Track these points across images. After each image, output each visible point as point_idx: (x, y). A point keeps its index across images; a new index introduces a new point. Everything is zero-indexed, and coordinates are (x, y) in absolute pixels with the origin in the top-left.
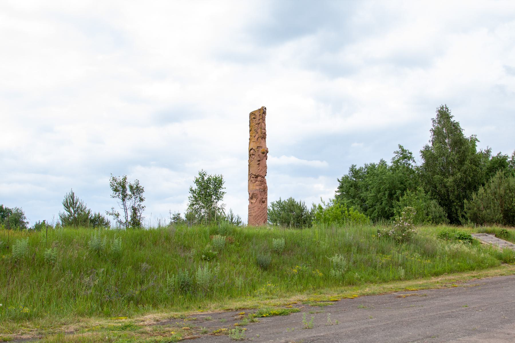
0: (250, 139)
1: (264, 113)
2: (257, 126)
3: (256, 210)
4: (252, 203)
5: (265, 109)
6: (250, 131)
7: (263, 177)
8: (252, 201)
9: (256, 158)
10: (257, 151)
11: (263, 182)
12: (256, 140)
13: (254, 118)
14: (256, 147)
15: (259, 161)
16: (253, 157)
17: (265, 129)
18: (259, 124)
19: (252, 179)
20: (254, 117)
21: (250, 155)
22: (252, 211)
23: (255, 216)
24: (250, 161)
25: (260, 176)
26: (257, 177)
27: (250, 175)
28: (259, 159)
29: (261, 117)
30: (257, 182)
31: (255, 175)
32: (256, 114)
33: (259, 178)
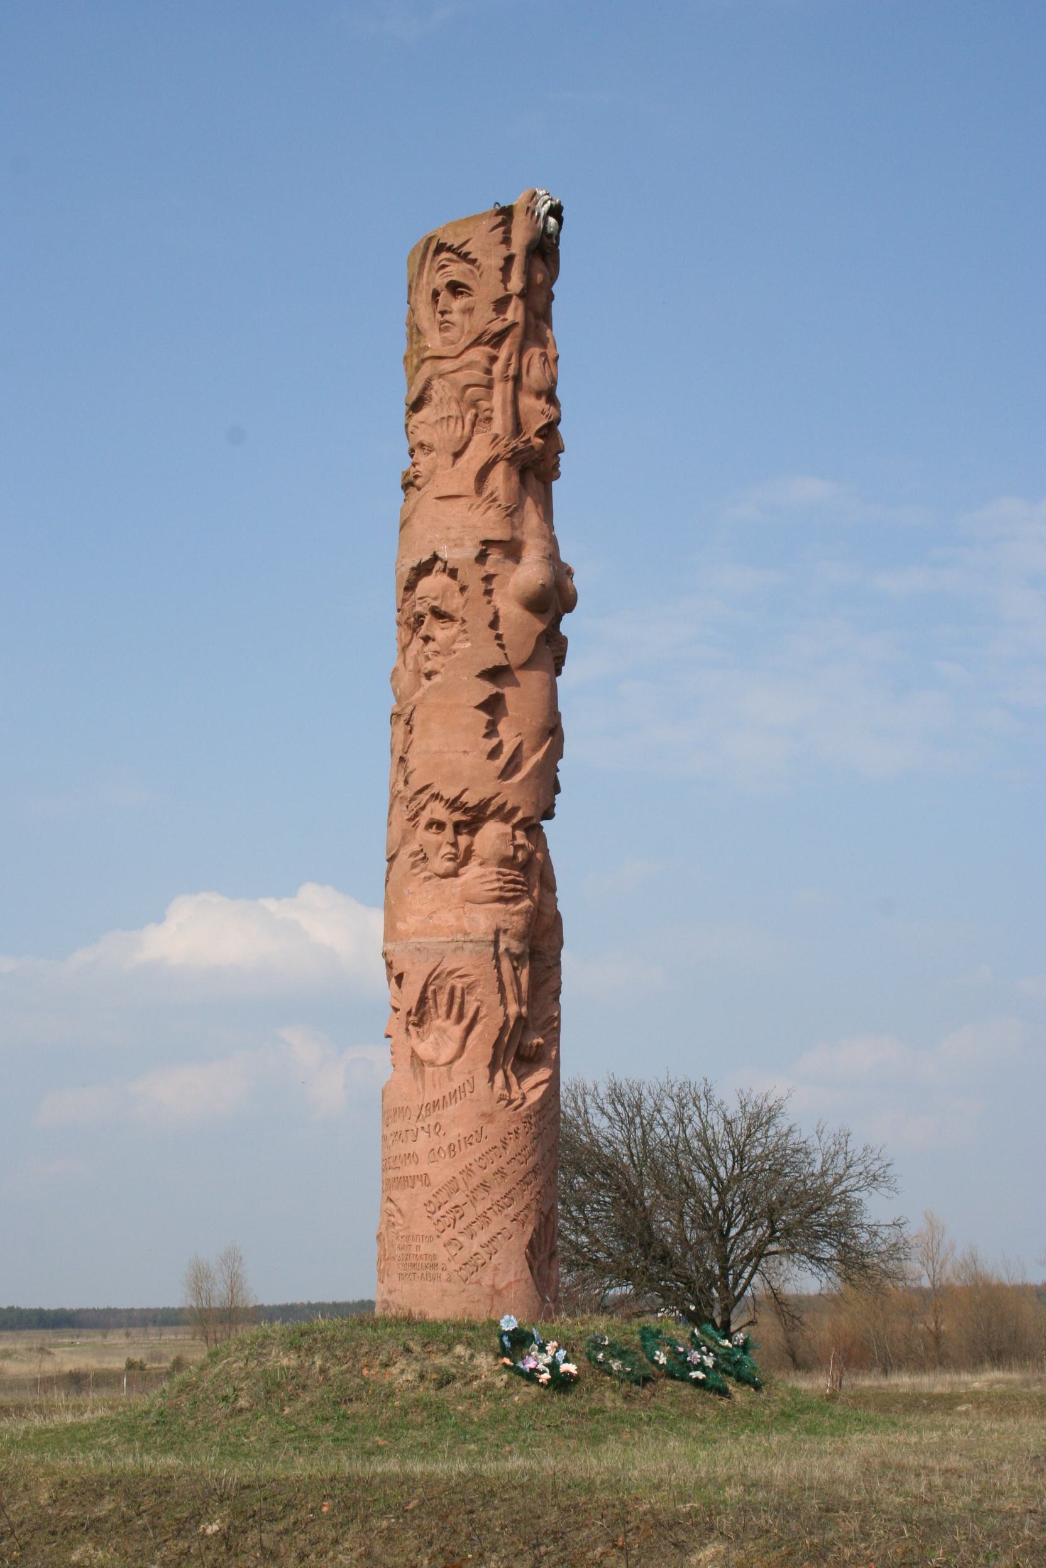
1: (544, 251)
2: (478, 354)
4: (418, 1062)
7: (532, 828)
8: (425, 1049)
9: (467, 649)
10: (476, 587)
15: (494, 674)
16: (441, 632)
17: (550, 396)
18: (498, 339)
19: (424, 837)
22: (422, 1144)
23: (452, 1187)
27: (411, 800)
28: (494, 658)
29: (516, 283)
30: (472, 870)
31: (454, 805)
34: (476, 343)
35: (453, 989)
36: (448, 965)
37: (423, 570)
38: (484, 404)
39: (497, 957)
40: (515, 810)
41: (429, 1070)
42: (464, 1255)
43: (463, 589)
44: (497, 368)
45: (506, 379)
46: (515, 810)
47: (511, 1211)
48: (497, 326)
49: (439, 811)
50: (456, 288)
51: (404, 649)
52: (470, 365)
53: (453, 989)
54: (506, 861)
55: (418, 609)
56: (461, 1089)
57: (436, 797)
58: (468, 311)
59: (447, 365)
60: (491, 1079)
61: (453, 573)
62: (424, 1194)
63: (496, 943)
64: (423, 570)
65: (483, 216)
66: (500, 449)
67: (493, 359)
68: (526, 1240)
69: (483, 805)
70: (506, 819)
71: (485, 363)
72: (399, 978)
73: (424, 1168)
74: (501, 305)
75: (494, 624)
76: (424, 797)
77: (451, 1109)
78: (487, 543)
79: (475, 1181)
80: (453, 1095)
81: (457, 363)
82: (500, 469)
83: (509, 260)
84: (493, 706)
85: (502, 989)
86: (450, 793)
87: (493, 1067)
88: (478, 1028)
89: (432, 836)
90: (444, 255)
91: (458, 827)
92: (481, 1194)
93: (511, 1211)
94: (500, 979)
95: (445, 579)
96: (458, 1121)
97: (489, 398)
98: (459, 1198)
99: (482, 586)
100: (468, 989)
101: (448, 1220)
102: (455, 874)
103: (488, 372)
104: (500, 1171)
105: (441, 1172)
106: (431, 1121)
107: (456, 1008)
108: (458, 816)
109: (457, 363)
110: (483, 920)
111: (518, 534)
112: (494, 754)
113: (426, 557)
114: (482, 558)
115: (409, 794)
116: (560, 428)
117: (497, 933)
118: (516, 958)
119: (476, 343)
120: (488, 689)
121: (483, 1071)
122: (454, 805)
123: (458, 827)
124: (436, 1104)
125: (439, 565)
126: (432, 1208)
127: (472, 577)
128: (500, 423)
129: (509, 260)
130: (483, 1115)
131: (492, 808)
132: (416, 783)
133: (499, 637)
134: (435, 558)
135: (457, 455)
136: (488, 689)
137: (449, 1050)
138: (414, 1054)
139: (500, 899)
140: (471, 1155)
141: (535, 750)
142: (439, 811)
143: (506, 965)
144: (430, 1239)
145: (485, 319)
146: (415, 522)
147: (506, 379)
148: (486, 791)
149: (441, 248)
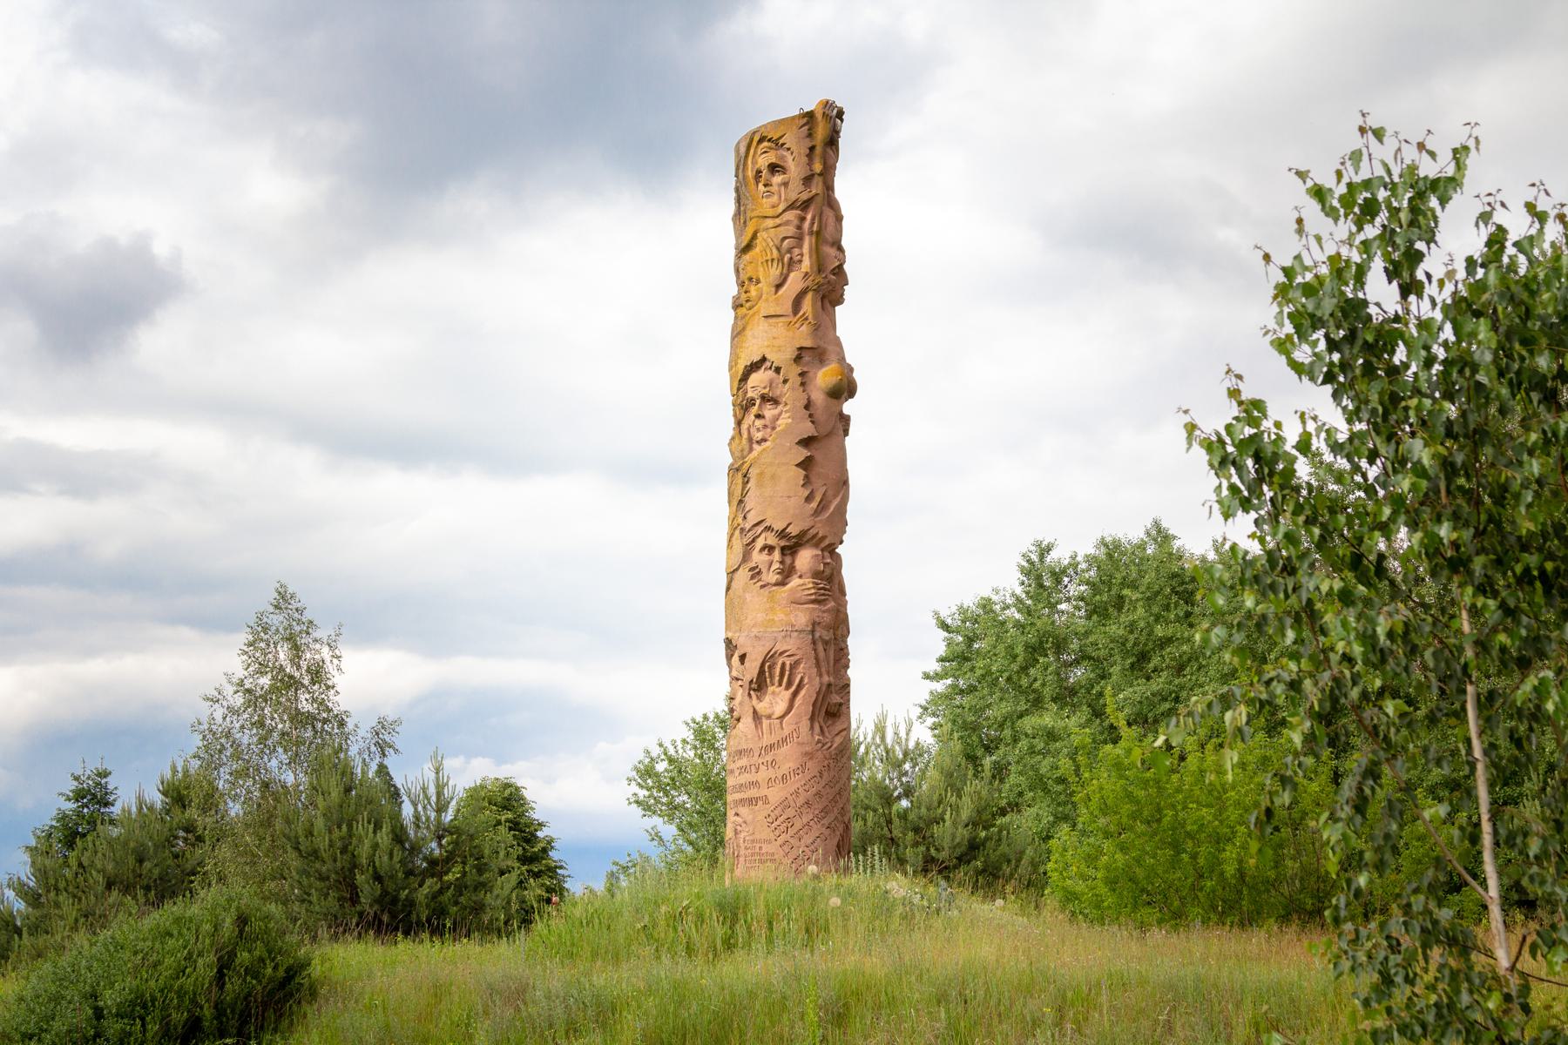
0: (737, 306)
2: (791, 215)
3: (785, 769)
5: (840, 114)
6: (745, 249)
7: (831, 550)
8: (762, 707)
10: (795, 380)
11: (830, 584)
12: (787, 307)
13: (774, 168)
14: (790, 353)
15: (806, 442)
16: (769, 412)
18: (805, 205)
19: (758, 558)
20: (771, 158)
21: (743, 407)
23: (784, 804)
24: (743, 442)
25: (815, 541)
26: (791, 546)
27: (744, 533)
28: (808, 429)
30: (795, 582)
31: (782, 534)
32: (789, 140)
33: (806, 558)
34: (791, 207)
35: (784, 664)
36: (780, 647)
37: (754, 367)
38: (796, 251)
39: (814, 642)
40: (824, 538)
41: (765, 722)
42: (794, 854)
43: (785, 381)
44: (806, 225)
45: (811, 233)
46: (824, 538)
47: (826, 822)
48: (805, 196)
49: (771, 540)
50: (774, 168)
51: (739, 423)
52: (787, 223)
53: (784, 664)
54: (817, 575)
55: (750, 394)
56: (790, 735)
57: (768, 528)
58: (785, 184)
59: (770, 223)
60: (812, 728)
61: (778, 370)
62: (762, 811)
63: (813, 631)
64: (754, 367)
65: (793, 118)
66: (809, 283)
67: (803, 219)
68: (835, 842)
69: (803, 533)
70: (816, 546)
71: (796, 222)
72: (743, 658)
73: (764, 792)
74: (807, 180)
75: (807, 407)
76: (760, 529)
77: (785, 749)
78: (800, 349)
79: (800, 801)
80: (784, 740)
81: (778, 221)
82: (809, 296)
83: (812, 149)
84: (806, 464)
85: (818, 665)
86: (779, 526)
87: (812, 719)
88: (803, 693)
89: (764, 557)
90: (766, 144)
91: (783, 549)
92: (804, 810)
93: (826, 822)
94: (817, 659)
95: (771, 373)
96: (788, 758)
97: (801, 247)
98: (790, 812)
99: (799, 379)
100: (794, 666)
101: (783, 828)
102: (782, 583)
103: (799, 227)
104: (818, 794)
105: (775, 794)
106: (769, 758)
107: (788, 678)
108: (783, 543)
109: (778, 221)
110: (802, 618)
111: (821, 343)
112: (809, 499)
113: (756, 358)
114: (798, 359)
115: (748, 526)
116: (845, 267)
117: (814, 624)
118: (826, 643)
119: (791, 207)
120: (803, 453)
121: (805, 723)
122: (782, 534)
123: (783, 549)
124: (772, 746)
125: (768, 364)
126: (771, 820)
127: (793, 372)
128: (806, 264)
129: (812, 149)
130: (806, 754)
131: (809, 536)
132: (753, 518)
133: (811, 416)
134: (764, 359)
135: (778, 287)
136: (803, 453)
137: (780, 708)
138: (755, 712)
139: (813, 602)
140: (796, 783)
141: (835, 496)
142: (771, 540)
143: (820, 647)
144: (769, 842)
145: (796, 192)
146: (748, 332)
147: (811, 233)
148: (805, 525)
149: (761, 140)
